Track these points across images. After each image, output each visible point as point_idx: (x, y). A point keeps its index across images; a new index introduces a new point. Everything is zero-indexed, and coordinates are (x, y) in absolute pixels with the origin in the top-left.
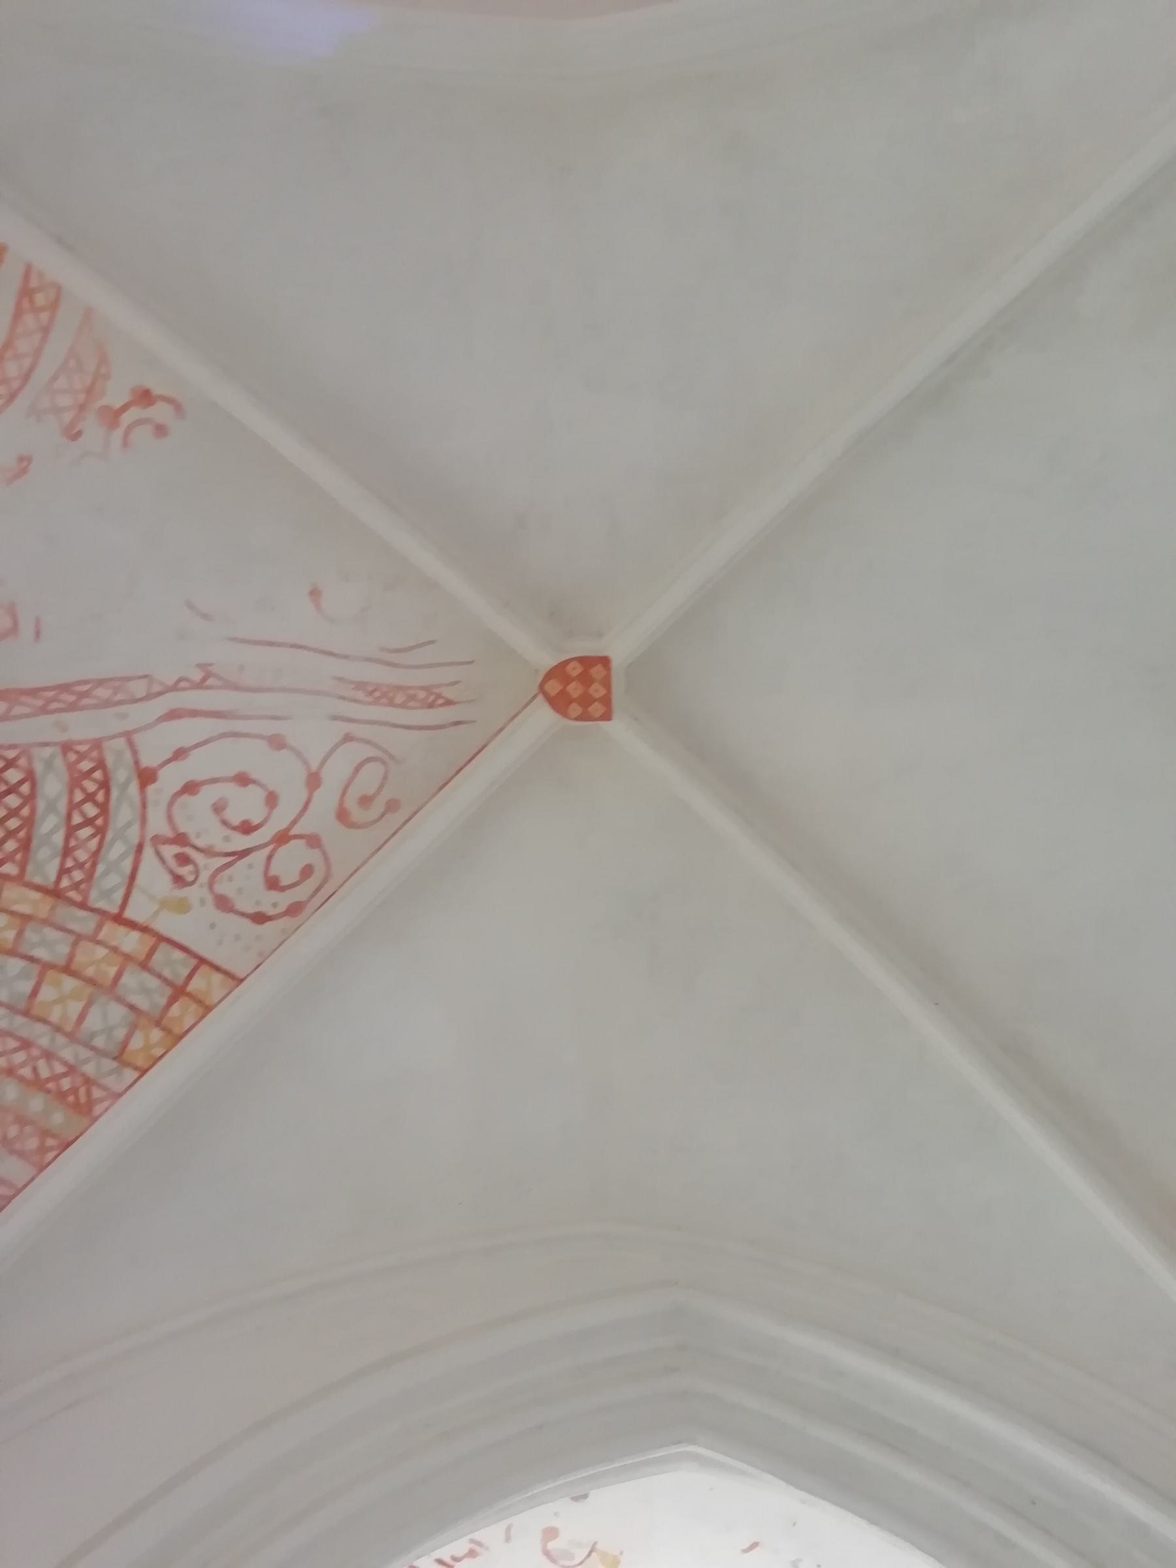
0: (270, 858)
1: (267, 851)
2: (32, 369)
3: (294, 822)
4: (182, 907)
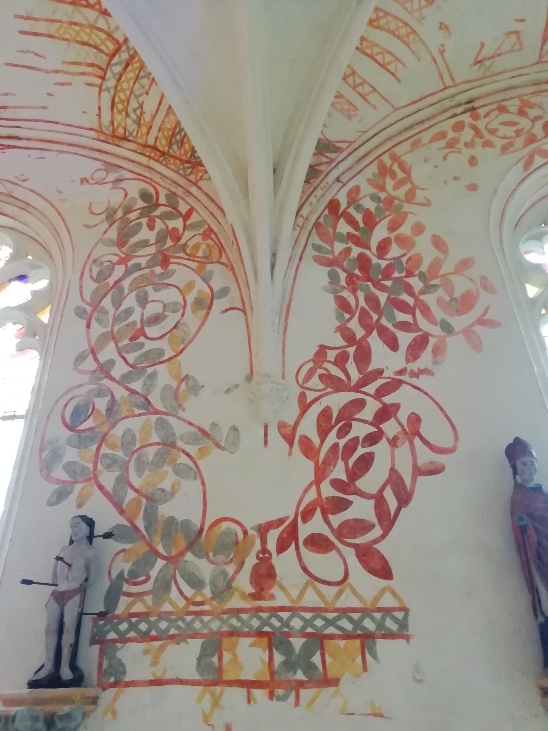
2: (403, 22)
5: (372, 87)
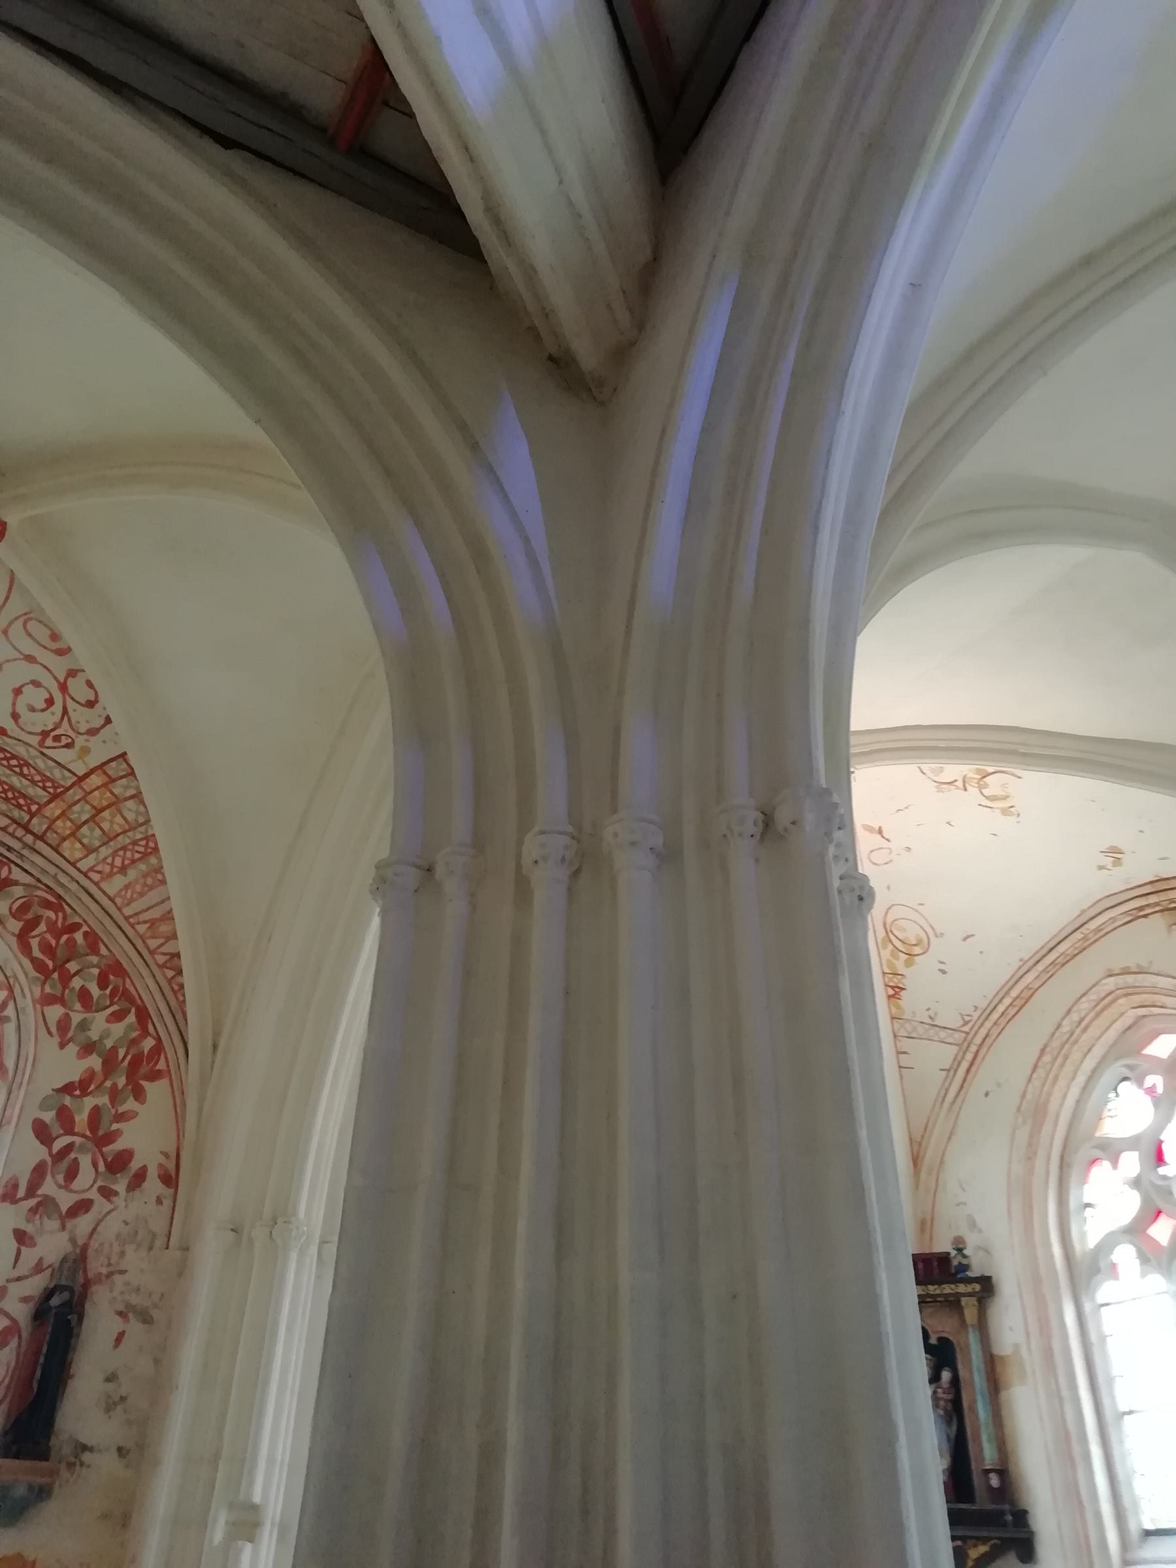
0: (73, 699)
1: (68, 698)
3: (55, 678)
4: (85, 751)
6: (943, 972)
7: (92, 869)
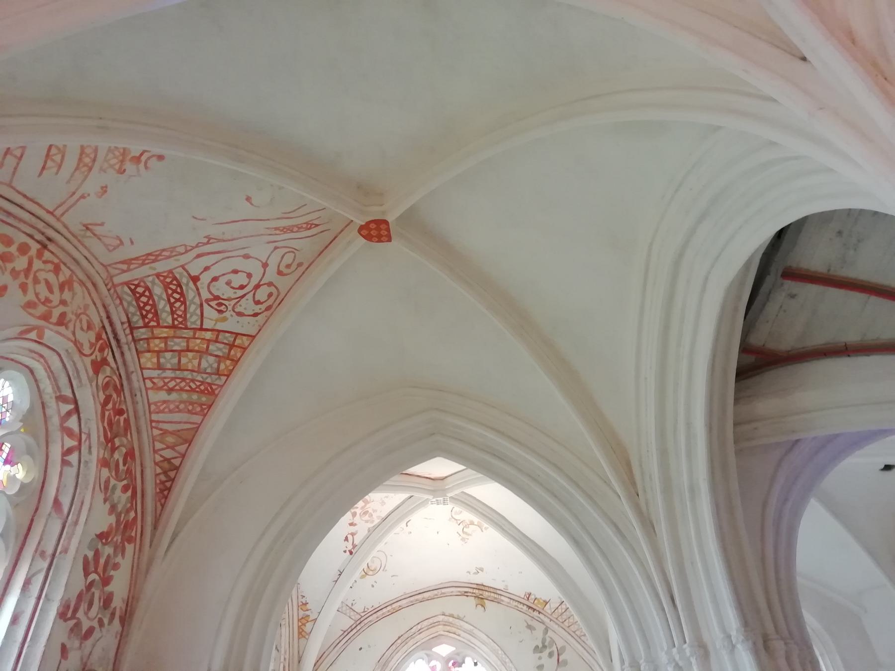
0: (254, 294)
1: (252, 292)
2: (96, 156)
3: (261, 280)
4: (225, 319)
5: (22, 156)
6: (373, 586)
7: (151, 379)
